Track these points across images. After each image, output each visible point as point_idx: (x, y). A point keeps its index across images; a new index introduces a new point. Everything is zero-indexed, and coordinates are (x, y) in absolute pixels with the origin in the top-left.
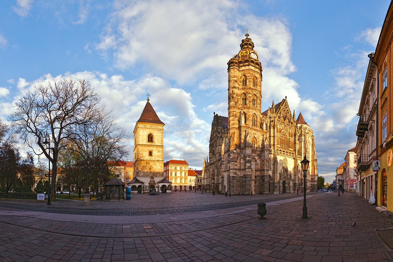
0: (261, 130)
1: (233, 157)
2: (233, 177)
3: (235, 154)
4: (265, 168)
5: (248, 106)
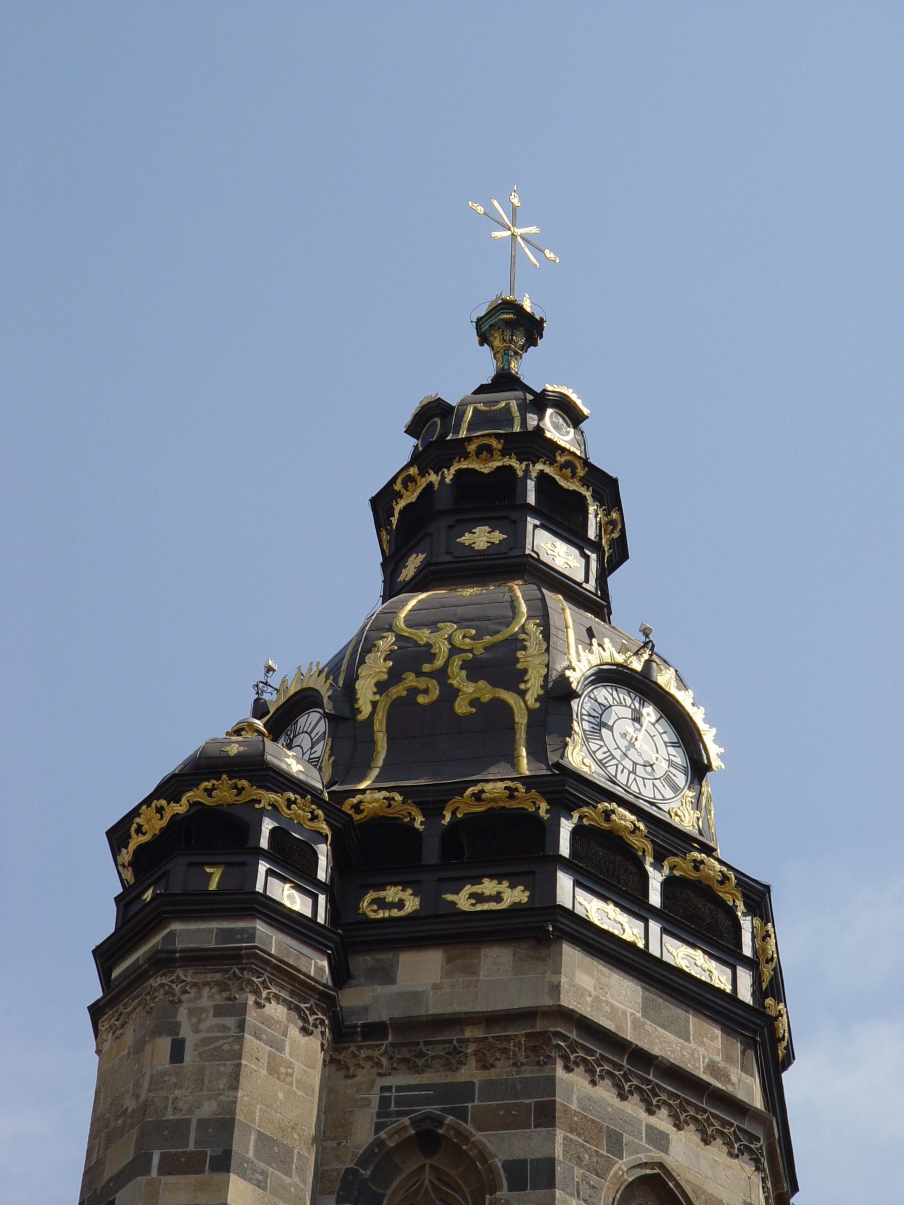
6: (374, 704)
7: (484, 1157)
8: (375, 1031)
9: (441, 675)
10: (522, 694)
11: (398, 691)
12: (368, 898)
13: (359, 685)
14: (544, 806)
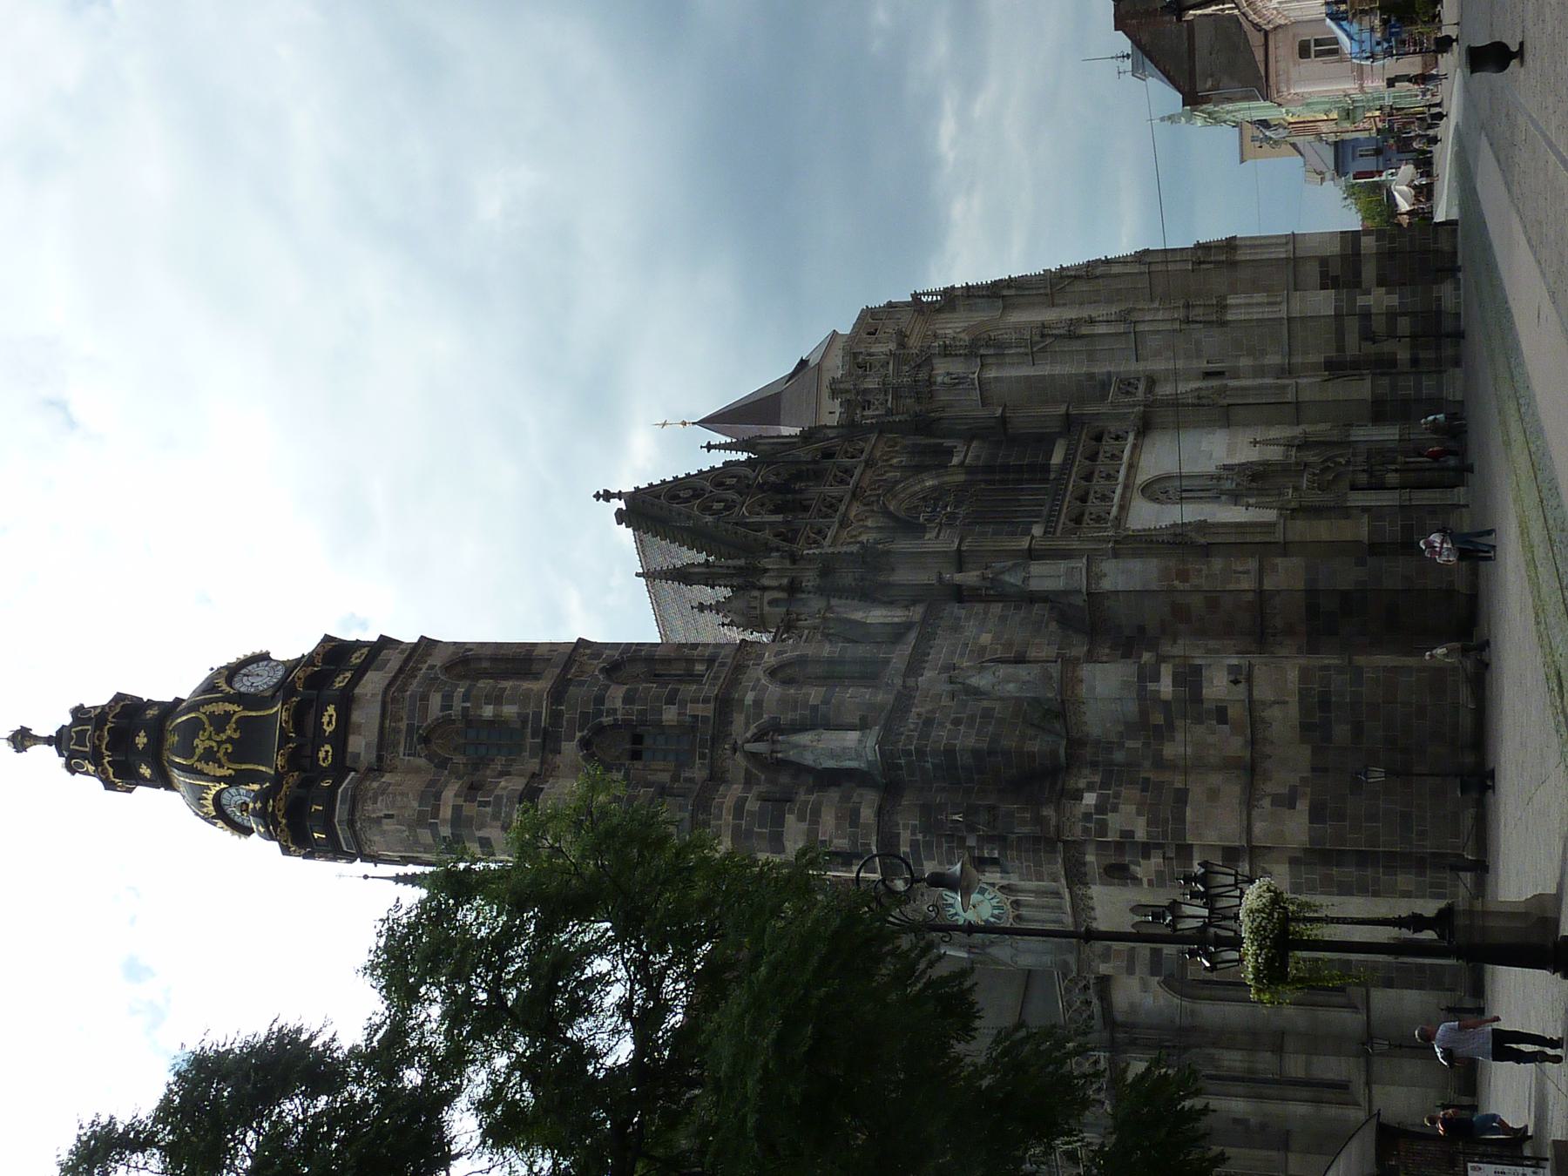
0: (912, 637)
1: (1139, 813)
2: (1316, 814)
3: (1117, 796)
4: (1245, 586)
5: (706, 710)
6: (228, 768)
7: (437, 719)
8: (380, 758)
9: (220, 743)
10: (235, 712)
11: (224, 760)
12: (324, 765)
13: (218, 774)
14: (294, 699)
